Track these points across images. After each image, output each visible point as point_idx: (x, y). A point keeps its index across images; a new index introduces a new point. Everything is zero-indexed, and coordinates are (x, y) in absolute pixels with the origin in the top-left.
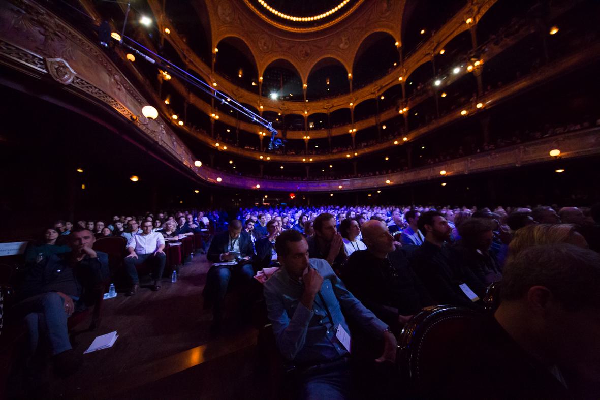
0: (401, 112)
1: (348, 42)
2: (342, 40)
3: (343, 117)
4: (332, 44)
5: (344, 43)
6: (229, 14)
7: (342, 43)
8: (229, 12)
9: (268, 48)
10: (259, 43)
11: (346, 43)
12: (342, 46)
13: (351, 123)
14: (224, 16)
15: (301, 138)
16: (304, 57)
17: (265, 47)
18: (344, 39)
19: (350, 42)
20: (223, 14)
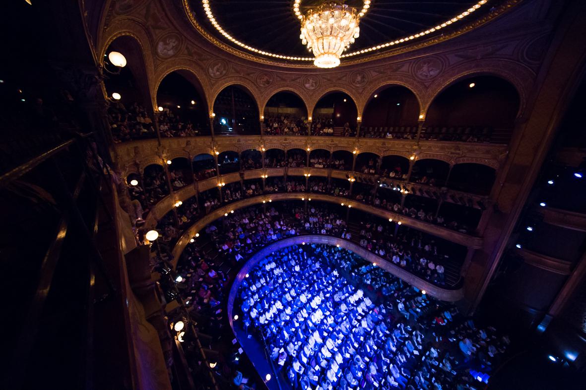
0: (349, 180)
2: (309, 80)
3: (299, 157)
4: (298, 80)
5: (310, 84)
6: (173, 47)
7: (309, 83)
9: (221, 74)
10: (210, 69)
11: (312, 86)
12: (307, 85)
13: (306, 166)
14: (165, 50)
15: (260, 177)
16: (264, 85)
17: (218, 73)
18: (311, 81)
19: (316, 86)
20: (165, 49)
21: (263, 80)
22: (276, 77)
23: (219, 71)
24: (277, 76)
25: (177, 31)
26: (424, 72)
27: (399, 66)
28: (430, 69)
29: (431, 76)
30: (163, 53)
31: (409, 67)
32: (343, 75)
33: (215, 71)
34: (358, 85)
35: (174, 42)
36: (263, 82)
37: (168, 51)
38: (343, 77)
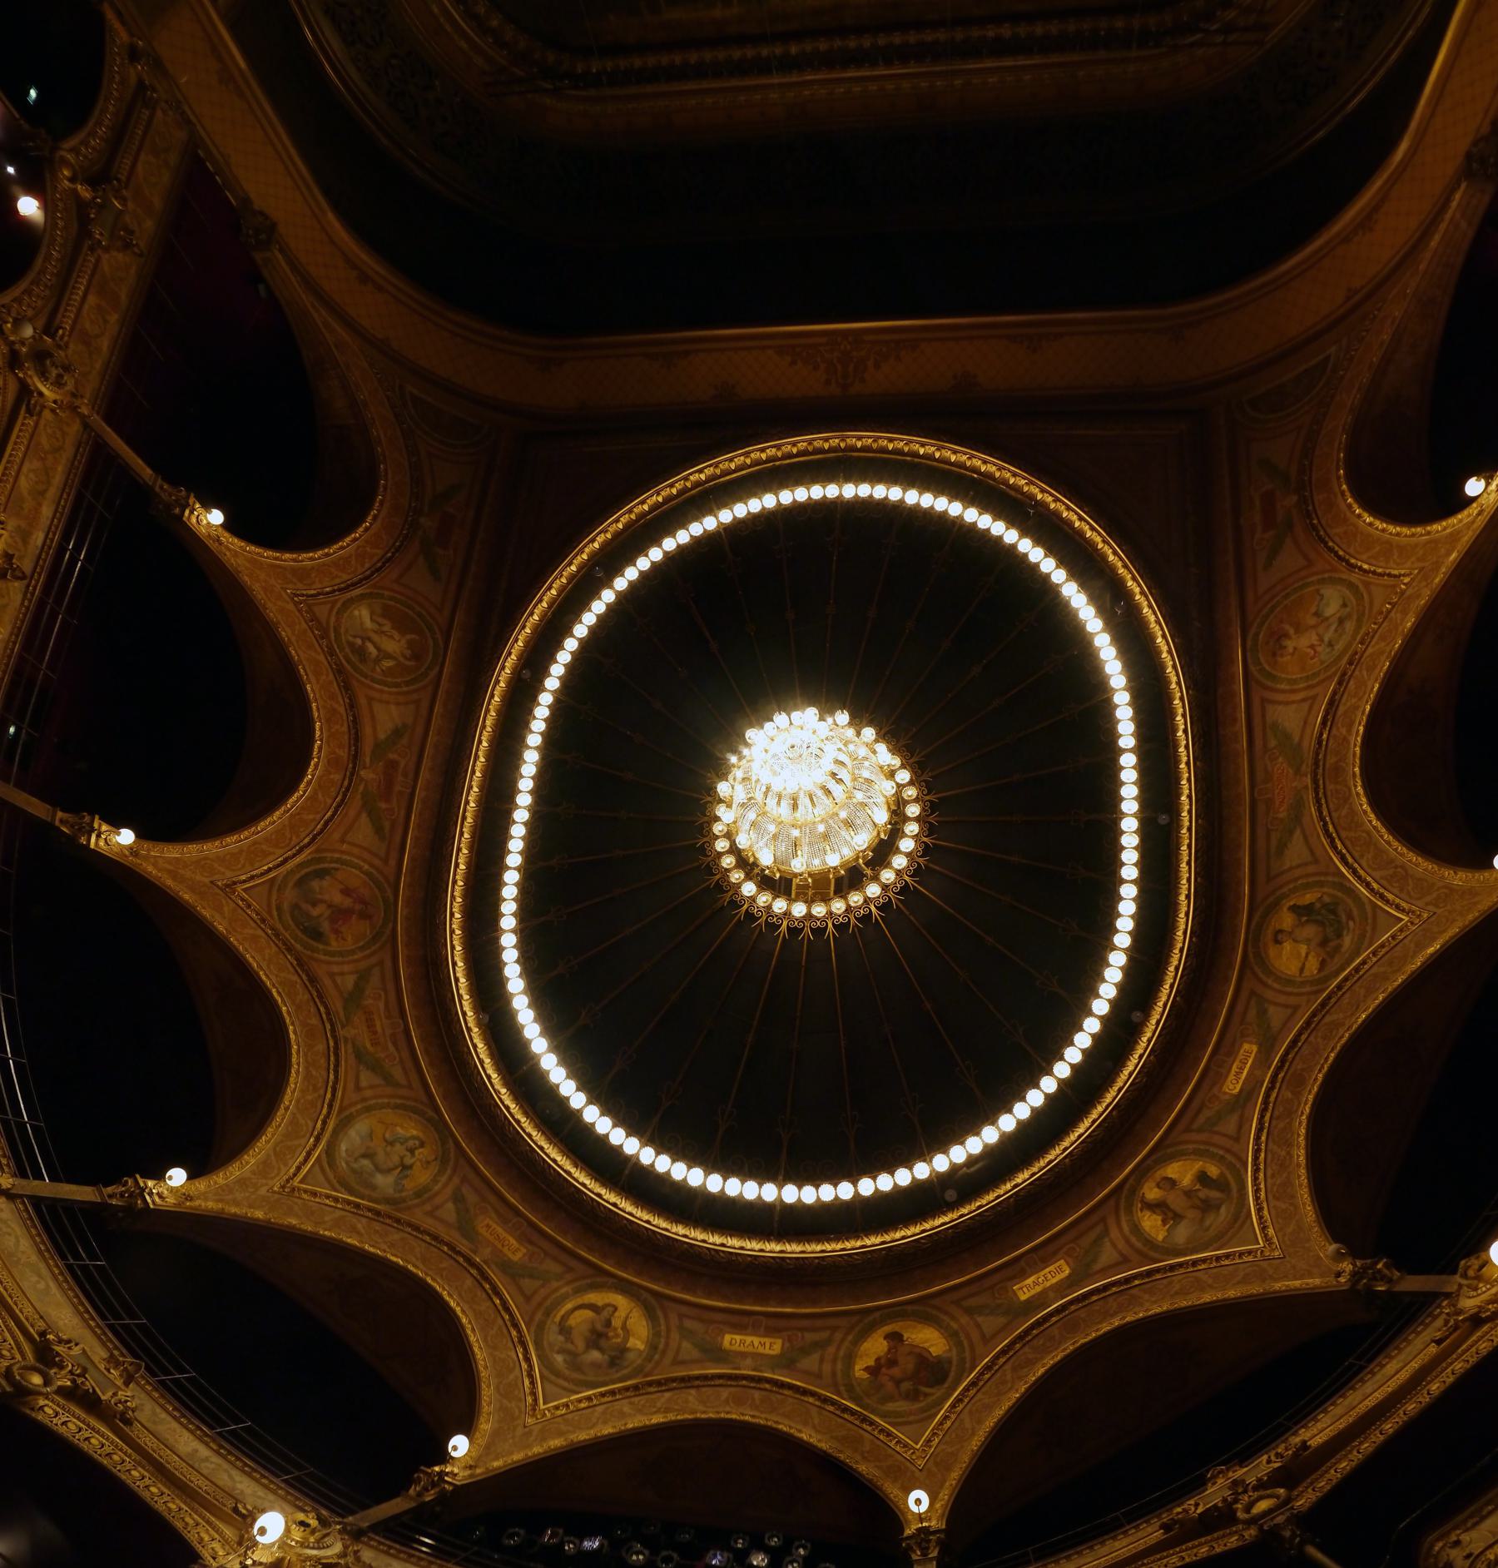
1: (1214, 1194)
5: (1191, 1214)
8: (408, 1161)
14: (365, 1162)
16: (913, 1396)
17: (595, 1355)
21: (896, 1372)
22: (964, 1320)
23: (603, 1343)
24: (969, 1311)
25: (431, 1113)
26: (1321, 640)
27: (1273, 743)
28: (1312, 621)
29: (1345, 605)
30: (355, 1166)
31: (1287, 703)
32: (1252, 1013)
33: (580, 1345)
34: (1347, 941)
35: (412, 1151)
36: (898, 1382)
37: (378, 1169)
38: (1262, 1012)
